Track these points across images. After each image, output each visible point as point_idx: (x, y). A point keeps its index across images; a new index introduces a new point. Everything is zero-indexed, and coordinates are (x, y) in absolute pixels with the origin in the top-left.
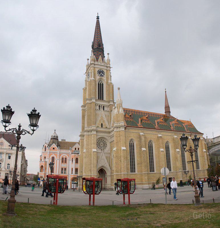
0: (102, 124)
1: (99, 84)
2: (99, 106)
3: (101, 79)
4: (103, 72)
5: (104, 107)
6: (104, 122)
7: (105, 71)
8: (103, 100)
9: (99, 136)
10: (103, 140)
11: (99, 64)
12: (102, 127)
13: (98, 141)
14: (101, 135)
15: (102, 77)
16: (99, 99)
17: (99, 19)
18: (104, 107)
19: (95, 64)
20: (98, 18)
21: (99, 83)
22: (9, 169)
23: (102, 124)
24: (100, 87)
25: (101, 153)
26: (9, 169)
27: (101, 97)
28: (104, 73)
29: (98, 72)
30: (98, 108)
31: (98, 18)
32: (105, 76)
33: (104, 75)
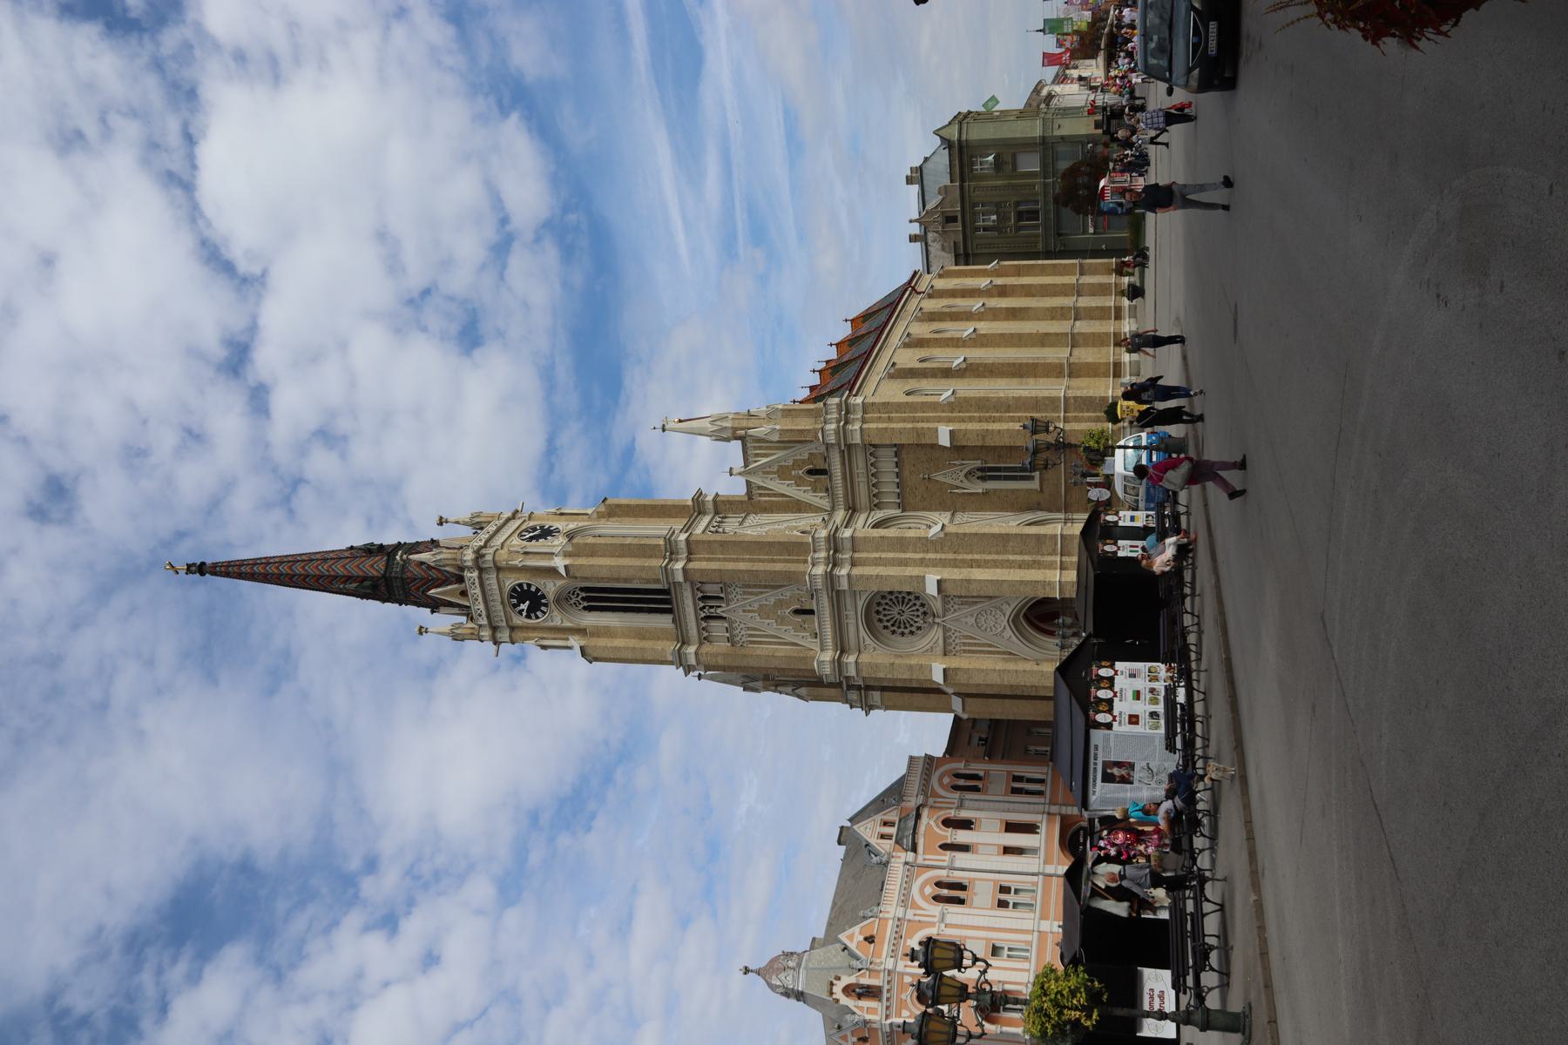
0: (797, 612)
1: (589, 609)
2: (707, 618)
3: (558, 601)
4: (514, 590)
5: (704, 598)
6: (780, 604)
7: (510, 582)
8: (666, 592)
9: (862, 633)
10: (879, 604)
11: (482, 607)
12: (811, 612)
13: (886, 627)
14: (855, 628)
15: (551, 597)
16: (669, 611)
17: (203, 564)
18: (704, 598)
19: (494, 629)
20: (201, 569)
21: (585, 608)
22: (1042, 781)
23: (797, 612)
24: (601, 597)
25: (946, 630)
26: (1042, 781)
27: (656, 600)
28: (520, 585)
29: (528, 617)
30: (717, 628)
31: (201, 569)
32: (537, 583)
33: (529, 586)
